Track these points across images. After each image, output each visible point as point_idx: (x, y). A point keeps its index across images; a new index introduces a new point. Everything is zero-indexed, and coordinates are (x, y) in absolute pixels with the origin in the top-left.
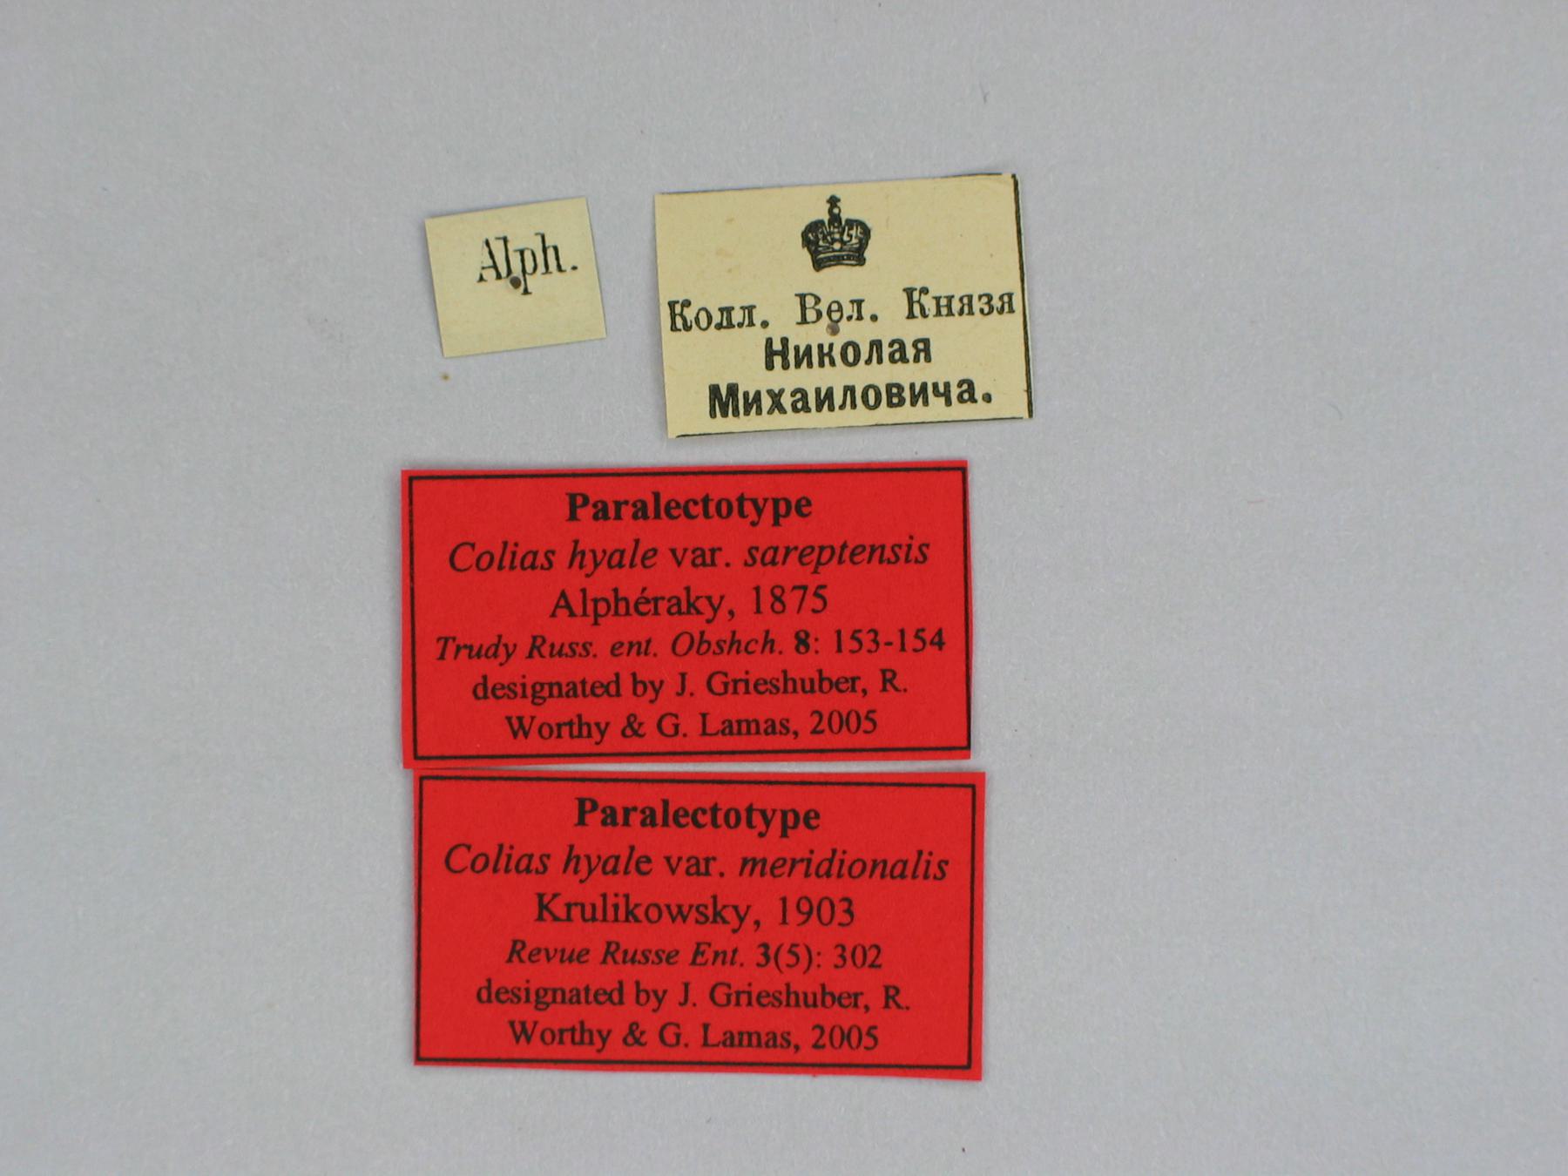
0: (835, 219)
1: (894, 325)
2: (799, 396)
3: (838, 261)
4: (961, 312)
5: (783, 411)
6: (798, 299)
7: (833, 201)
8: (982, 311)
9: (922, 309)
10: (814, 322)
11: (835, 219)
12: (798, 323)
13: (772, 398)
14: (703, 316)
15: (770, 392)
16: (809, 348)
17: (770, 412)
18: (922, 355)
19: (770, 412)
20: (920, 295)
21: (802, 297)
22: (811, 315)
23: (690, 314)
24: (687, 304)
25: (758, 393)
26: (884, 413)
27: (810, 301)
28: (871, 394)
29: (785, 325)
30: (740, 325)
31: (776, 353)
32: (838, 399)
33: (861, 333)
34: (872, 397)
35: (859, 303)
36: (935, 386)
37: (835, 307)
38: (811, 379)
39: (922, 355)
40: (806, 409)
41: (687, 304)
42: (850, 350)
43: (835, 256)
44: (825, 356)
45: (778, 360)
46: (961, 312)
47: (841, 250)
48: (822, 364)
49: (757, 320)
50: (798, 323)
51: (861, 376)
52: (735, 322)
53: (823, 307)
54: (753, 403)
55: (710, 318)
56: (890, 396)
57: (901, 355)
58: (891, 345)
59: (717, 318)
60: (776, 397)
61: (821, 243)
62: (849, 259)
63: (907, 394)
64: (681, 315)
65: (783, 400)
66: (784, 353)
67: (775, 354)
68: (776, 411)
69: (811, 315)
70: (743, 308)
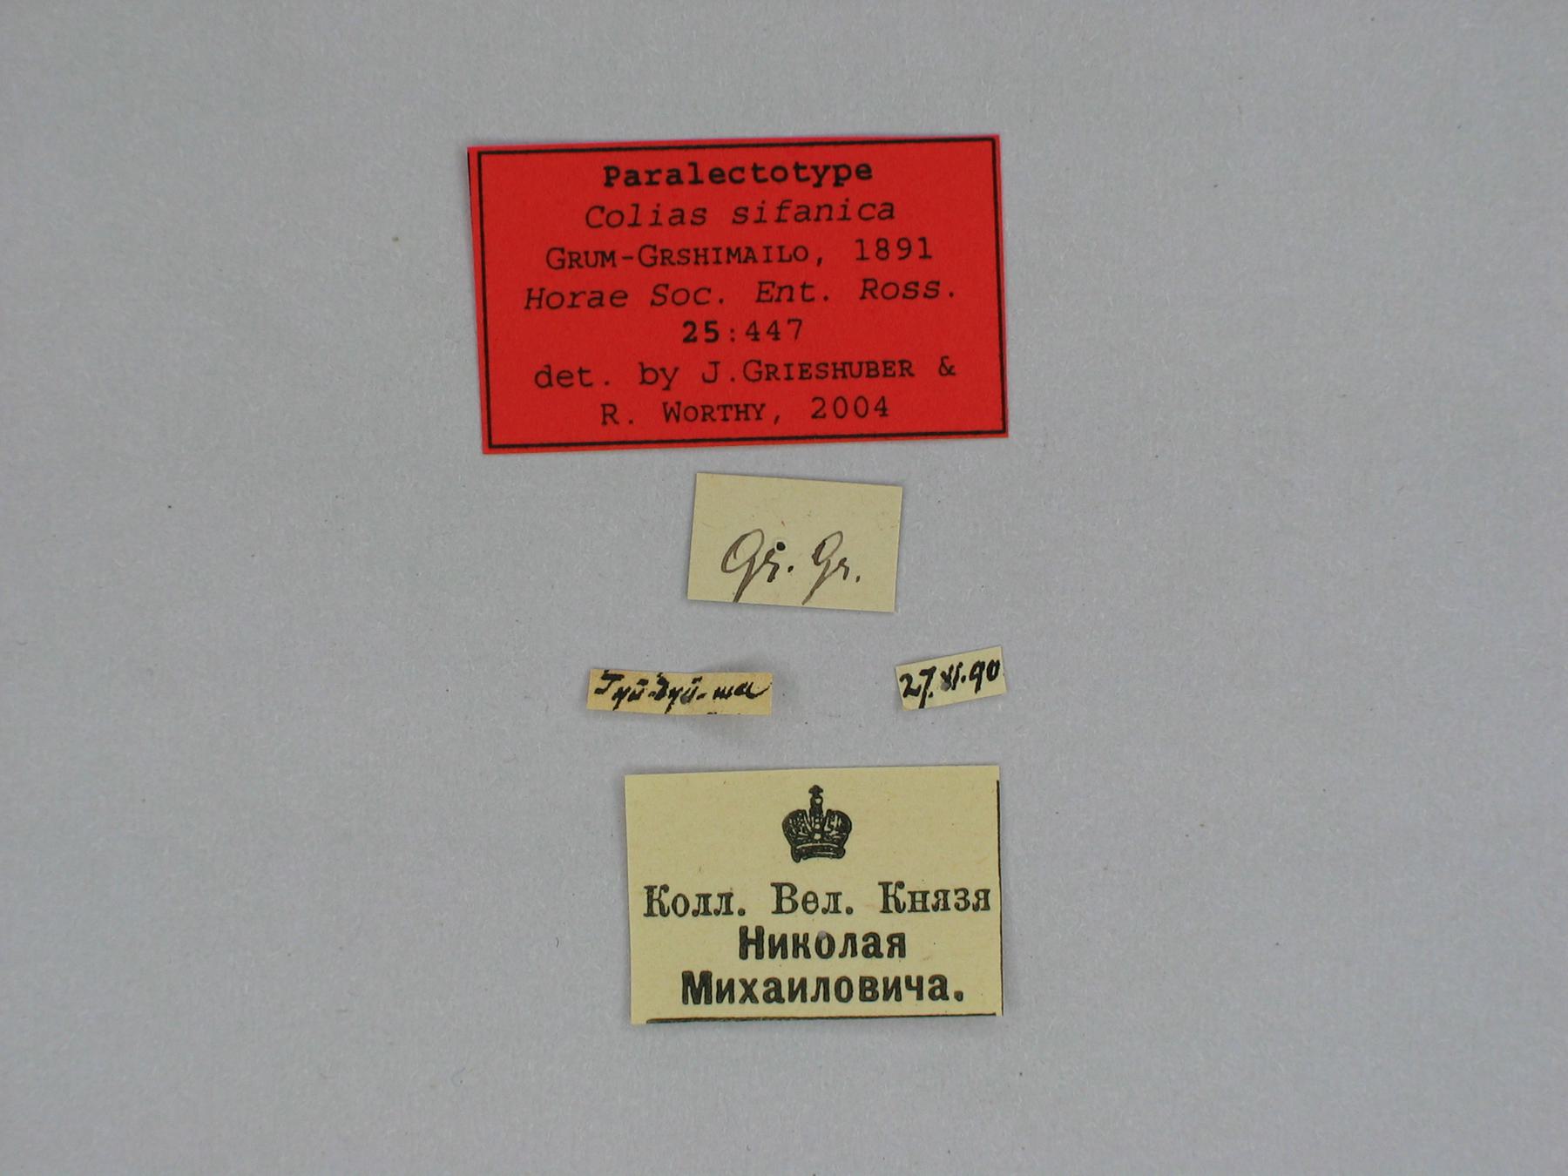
23: (667, 899)
31: (751, 942)
36: (908, 979)
44: (800, 945)
45: (752, 949)
57: (875, 950)
63: (880, 988)
67: (751, 942)
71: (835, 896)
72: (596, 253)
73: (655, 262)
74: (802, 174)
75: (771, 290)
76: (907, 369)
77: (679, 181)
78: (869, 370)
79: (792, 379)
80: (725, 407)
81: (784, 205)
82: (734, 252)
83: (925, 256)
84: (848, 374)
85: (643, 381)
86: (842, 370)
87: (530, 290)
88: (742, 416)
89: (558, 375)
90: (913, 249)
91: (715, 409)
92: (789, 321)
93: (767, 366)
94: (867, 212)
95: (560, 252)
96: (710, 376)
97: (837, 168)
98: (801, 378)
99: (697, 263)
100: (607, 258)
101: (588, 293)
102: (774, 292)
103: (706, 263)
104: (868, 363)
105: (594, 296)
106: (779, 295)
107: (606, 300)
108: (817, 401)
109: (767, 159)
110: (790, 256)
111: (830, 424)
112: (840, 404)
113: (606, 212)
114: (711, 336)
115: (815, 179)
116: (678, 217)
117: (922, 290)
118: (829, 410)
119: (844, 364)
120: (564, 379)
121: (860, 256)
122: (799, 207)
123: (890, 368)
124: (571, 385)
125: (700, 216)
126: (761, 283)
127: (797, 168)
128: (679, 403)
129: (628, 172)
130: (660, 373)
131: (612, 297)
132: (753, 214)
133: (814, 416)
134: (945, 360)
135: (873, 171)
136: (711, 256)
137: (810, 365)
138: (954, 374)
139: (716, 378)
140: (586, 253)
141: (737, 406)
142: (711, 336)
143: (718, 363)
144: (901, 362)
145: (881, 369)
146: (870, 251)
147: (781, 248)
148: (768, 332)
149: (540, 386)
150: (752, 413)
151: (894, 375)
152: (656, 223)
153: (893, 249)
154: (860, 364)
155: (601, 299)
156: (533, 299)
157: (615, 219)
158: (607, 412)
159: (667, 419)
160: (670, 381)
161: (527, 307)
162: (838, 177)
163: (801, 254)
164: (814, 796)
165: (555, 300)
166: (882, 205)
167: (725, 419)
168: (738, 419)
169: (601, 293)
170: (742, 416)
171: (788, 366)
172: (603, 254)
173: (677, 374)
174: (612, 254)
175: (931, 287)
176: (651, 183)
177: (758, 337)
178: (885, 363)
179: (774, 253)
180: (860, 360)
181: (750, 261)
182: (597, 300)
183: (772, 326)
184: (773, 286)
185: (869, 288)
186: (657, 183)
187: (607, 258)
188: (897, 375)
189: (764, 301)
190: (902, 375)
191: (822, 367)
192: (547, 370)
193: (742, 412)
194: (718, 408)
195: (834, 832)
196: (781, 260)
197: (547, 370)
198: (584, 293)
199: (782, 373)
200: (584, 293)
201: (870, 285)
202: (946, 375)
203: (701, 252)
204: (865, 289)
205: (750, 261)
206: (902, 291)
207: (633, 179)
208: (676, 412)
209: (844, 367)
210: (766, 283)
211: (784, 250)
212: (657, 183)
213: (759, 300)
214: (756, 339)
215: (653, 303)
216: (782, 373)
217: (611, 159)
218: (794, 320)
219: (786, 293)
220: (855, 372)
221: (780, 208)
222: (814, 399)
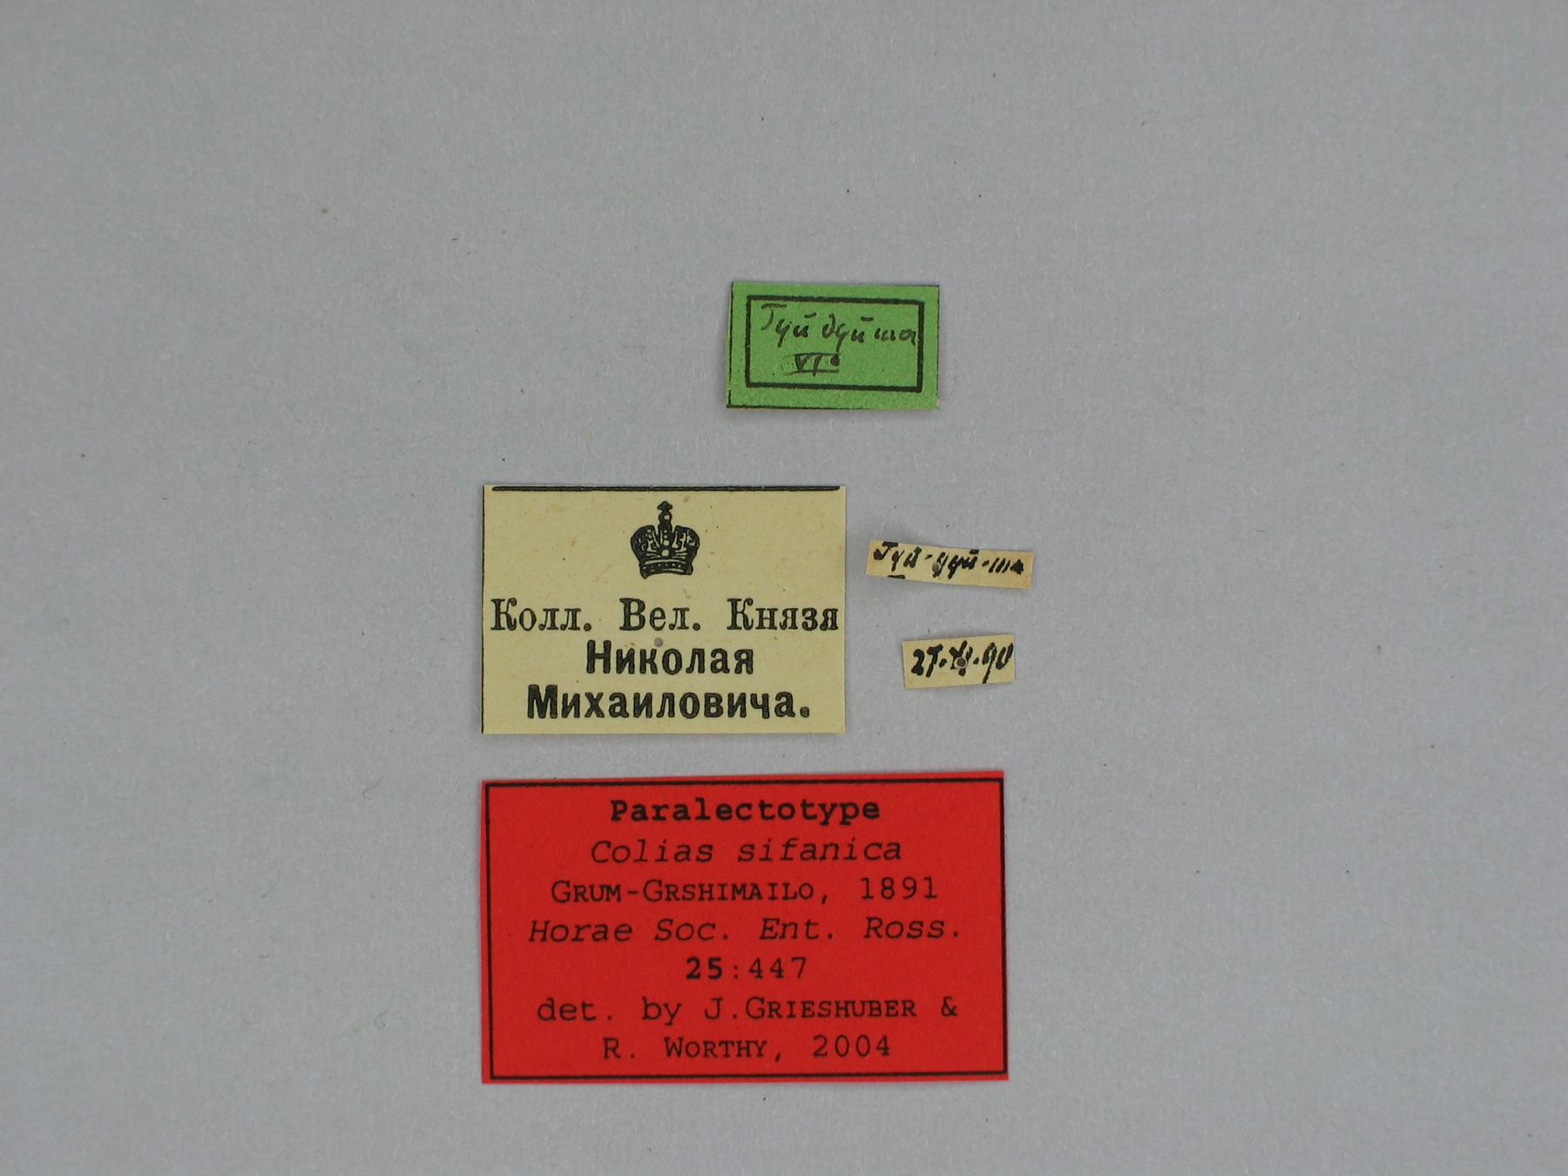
0: (665, 524)
1: (716, 634)
2: (617, 700)
3: (659, 569)
11: (665, 524)
13: (591, 702)
18: (744, 666)
20: (744, 606)
21: (627, 602)
22: (635, 621)
27: (634, 607)
29: (607, 627)
33: (685, 643)
35: (683, 611)
38: (632, 684)
39: (744, 666)
42: (672, 659)
47: (669, 557)
48: (643, 670)
49: (580, 624)
51: (680, 684)
52: (558, 625)
55: (534, 620)
58: (714, 654)
61: (649, 549)
65: (601, 704)
69: (635, 621)
72: (601, 887)
73: (661, 897)
74: (810, 811)
75: (775, 930)
76: (910, 1009)
77: (687, 817)
78: (872, 1009)
79: (795, 1016)
80: (726, 1043)
81: (792, 842)
82: (739, 887)
83: (930, 896)
84: (850, 1010)
85: (646, 1017)
86: (845, 1008)
87: (535, 923)
88: (744, 1052)
89: (565, 1005)
90: (918, 888)
91: (717, 1045)
92: (793, 959)
93: (770, 1004)
94: (872, 852)
95: (565, 885)
96: (713, 1013)
97: (844, 806)
98: (804, 1016)
99: (701, 898)
100: (612, 891)
101: (593, 928)
102: (778, 929)
103: (711, 898)
104: (871, 1002)
105: (598, 929)
106: (783, 934)
107: (611, 934)
108: (818, 1040)
109: (774, 796)
110: (796, 893)
111: (832, 1063)
112: (842, 1043)
113: (613, 847)
114: (715, 972)
115: (821, 817)
116: (684, 853)
117: (926, 929)
118: (830, 1048)
119: (846, 1003)
120: (567, 1012)
121: (865, 894)
122: (805, 846)
123: (893, 1008)
124: (574, 1018)
125: (707, 852)
126: (765, 920)
127: (805, 805)
128: (681, 1039)
129: (635, 807)
130: (664, 1011)
131: (616, 932)
132: (759, 851)
133: (816, 1054)
134: (948, 1001)
135: (880, 811)
136: (717, 892)
137: (813, 1003)
138: (955, 1015)
139: (718, 1015)
140: (592, 887)
141: (739, 1043)
142: (715, 972)
143: (721, 999)
144: (904, 1002)
145: (884, 1009)
146: (876, 888)
147: (786, 885)
148: (772, 970)
149: (541, 1017)
150: (753, 1047)
151: (897, 1014)
152: (662, 859)
153: (898, 887)
154: (863, 1003)
155: (605, 934)
156: (539, 931)
157: (621, 854)
158: (609, 1046)
159: (669, 1054)
160: (672, 1016)
161: (532, 939)
162: (845, 815)
163: (806, 891)
165: (559, 934)
166: (889, 845)
167: (727, 1055)
168: (739, 1055)
169: (606, 927)
170: (744, 1052)
171: (791, 1003)
172: (609, 888)
173: (680, 1008)
174: (618, 887)
175: (935, 925)
176: (658, 817)
177: (761, 974)
178: (887, 1002)
179: (780, 891)
180: (863, 1000)
181: (755, 897)
182: (601, 934)
183: (775, 964)
184: (778, 923)
185: (874, 927)
186: (664, 819)
187: (612, 891)
188: (900, 1014)
189: (767, 938)
190: (904, 1015)
191: (825, 1006)
192: (550, 1003)
193: (744, 1048)
194: (720, 1045)
196: (786, 898)
197: (550, 1003)
198: (589, 926)
199: (785, 1010)
200: (589, 926)
201: (874, 923)
202: (947, 1015)
203: (706, 888)
204: (869, 928)
205: (755, 897)
206: (907, 929)
207: (640, 813)
208: (678, 1046)
209: (846, 1006)
210: (770, 919)
211: (789, 888)
212: (664, 819)
213: (763, 937)
214: (759, 976)
215: (657, 938)
216: (785, 1010)
217: (615, 793)
218: (798, 958)
219: (790, 931)
220: (859, 1011)
221: (787, 845)
222: (815, 1038)
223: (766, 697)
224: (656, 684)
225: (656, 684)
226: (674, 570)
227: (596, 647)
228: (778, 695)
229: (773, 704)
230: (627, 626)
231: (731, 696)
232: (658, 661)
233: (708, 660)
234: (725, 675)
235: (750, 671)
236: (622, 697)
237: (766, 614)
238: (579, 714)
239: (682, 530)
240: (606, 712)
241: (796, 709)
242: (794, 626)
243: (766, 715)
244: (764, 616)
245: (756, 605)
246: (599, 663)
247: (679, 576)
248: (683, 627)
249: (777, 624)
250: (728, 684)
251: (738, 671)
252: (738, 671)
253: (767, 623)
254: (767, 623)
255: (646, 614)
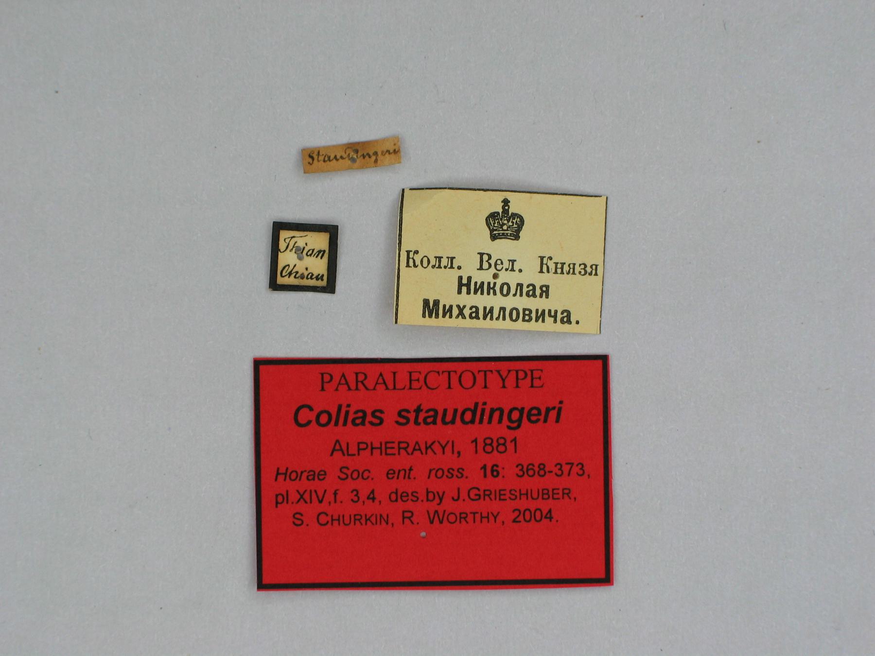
1: (531, 276)
2: (474, 310)
4: (568, 273)
5: (464, 317)
6: (479, 256)
7: (506, 202)
8: (580, 272)
9: (548, 268)
10: (486, 270)
12: (478, 269)
14: (425, 261)
15: (458, 306)
16: (483, 283)
17: (457, 317)
18: (544, 294)
19: (457, 317)
21: (481, 255)
24: (416, 252)
25: (451, 307)
26: (520, 325)
27: (485, 258)
28: (514, 312)
29: (470, 269)
30: (445, 267)
32: (496, 314)
33: (514, 279)
34: (515, 315)
35: (513, 261)
37: (499, 262)
38: (482, 301)
39: (544, 294)
40: (477, 317)
41: (416, 252)
42: (505, 287)
43: (503, 234)
46: (568, 273)
48: (488, 294)
49: (455, 265)
50: (478, 269)
51: (510, 302)
52: (442, 265)
53: (492, 262)
54: (448, 312)
56: (524, 315)
58: (528, 287)
59: (433, 262)
60: (461, 310)
62: (510, 236)
64: (413, 258)
66: (468, 285)
68: (460, 316)
69: (486, 265)
70: (448, 258)
71: (513, 262)
164: (505, 204)
195: (515, 226)
223: (556, 312)
224: (496, 301)
225: (496, 301)
226: (509, 237)
227: (463, 280)
228: (562, 312)
229: (559, 316)
230: (481, 268)
231: (537, 311)
232: (497, 288)
233: (525, 290)
234: (534, 298)
235: (547, 297)
236: (477, 308)
237: (559, 266)
238: (452, 315)
239: (515, 215)
240: (467, 315)
241: (573, 319)
242: (574, 273)
243: (555, 321)
244: (558, 267)
245: (554, 260)
246: (464, 289)
247: (512, 241)
248: (513, 270)
249: (565, 271)
250: (536, 304)
251: (541, 296)
252: (541, 296)
253: (559, 271)
254: (559, 271)
255: (492, 262)
